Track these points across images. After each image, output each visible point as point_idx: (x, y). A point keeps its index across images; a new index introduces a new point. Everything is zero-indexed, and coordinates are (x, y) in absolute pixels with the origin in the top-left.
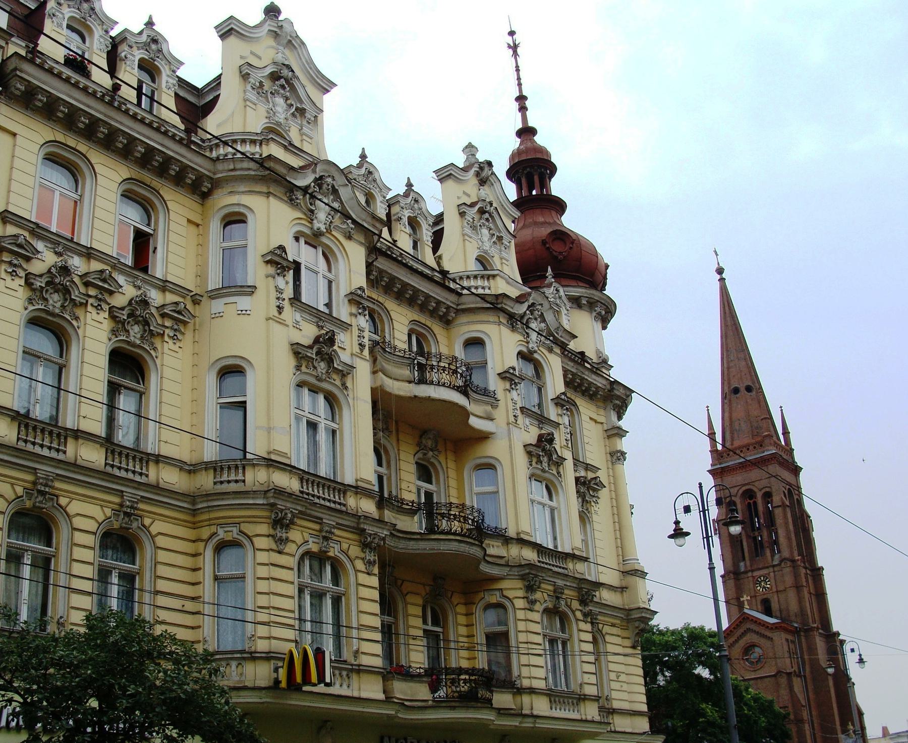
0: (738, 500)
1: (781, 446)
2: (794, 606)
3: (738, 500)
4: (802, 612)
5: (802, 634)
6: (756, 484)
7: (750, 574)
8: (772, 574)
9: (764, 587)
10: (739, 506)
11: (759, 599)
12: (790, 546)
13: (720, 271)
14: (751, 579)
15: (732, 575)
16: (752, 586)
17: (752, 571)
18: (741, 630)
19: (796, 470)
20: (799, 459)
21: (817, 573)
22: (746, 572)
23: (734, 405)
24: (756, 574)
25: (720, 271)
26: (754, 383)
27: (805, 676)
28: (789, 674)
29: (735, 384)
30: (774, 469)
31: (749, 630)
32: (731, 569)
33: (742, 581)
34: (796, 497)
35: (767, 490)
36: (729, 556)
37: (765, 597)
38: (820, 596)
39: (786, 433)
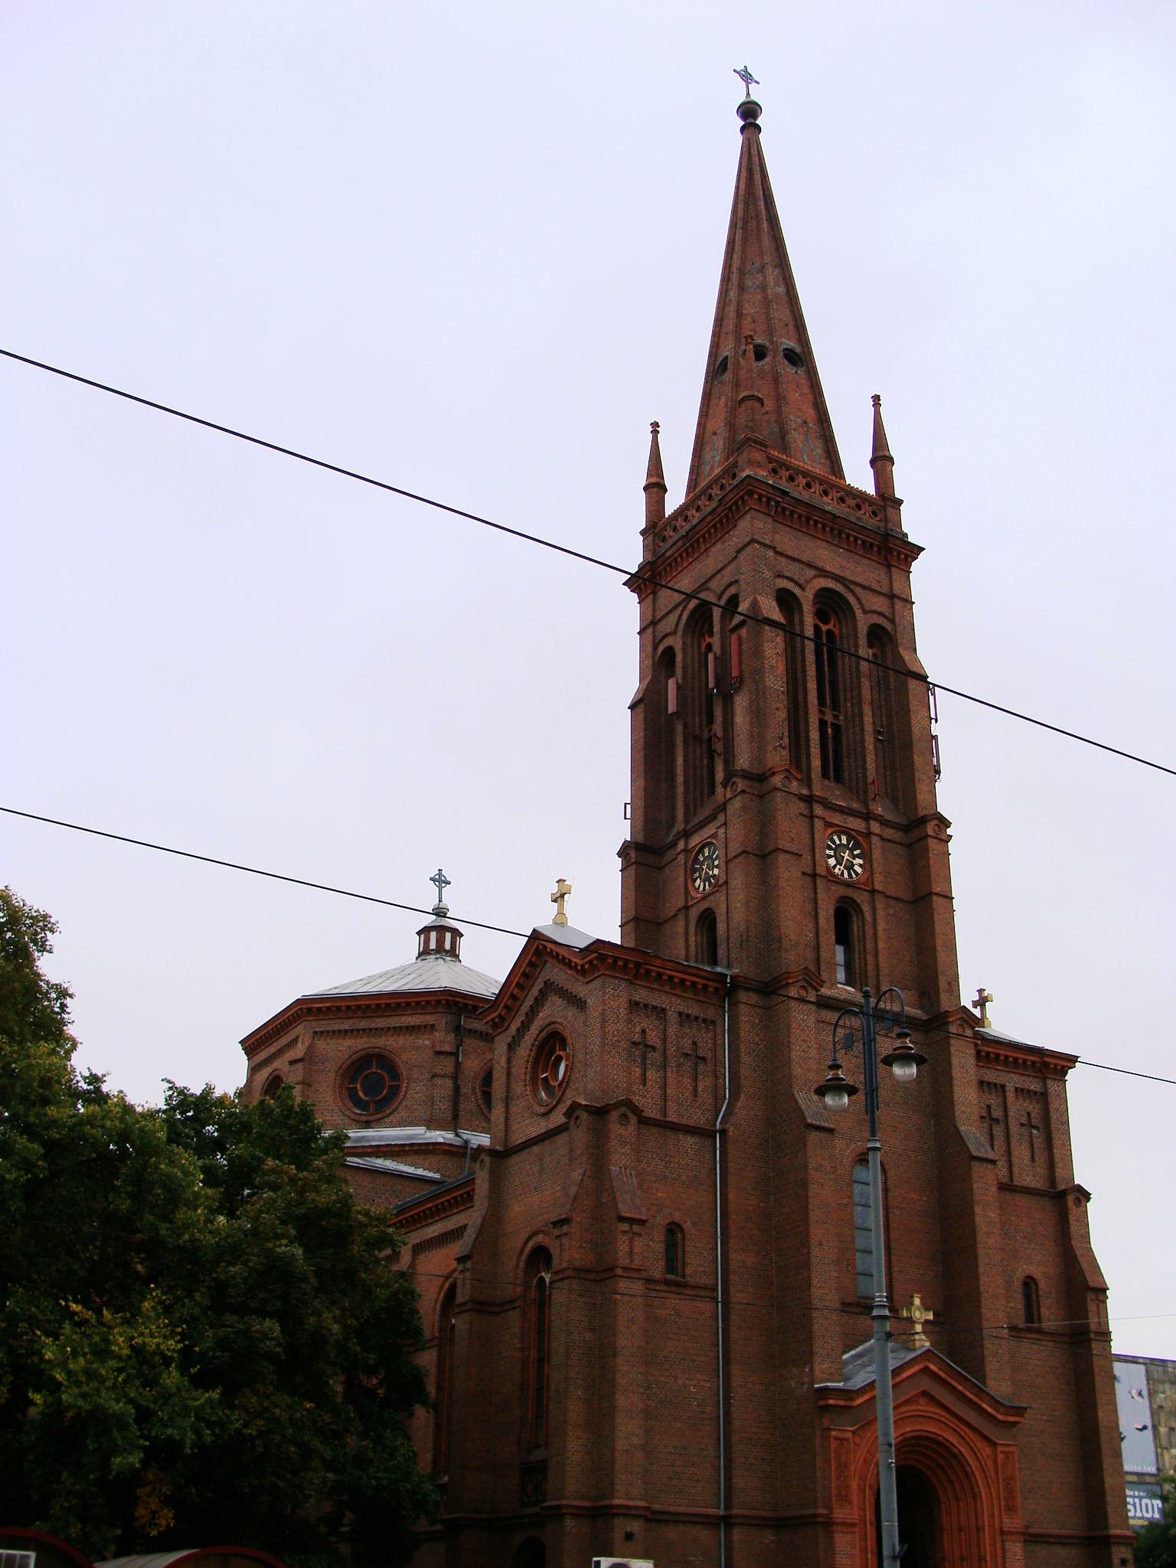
0: (676, 642)
1: (860, 496)
2: (736, 913)
3: (676, 642)
4: (766, 934)
5: (743, 996)
6: (713, 584)
7: (681, 845)
8: (722, 831)
9: (707, 879)
10: (679, 658)
11: (694, 914)
12: (758, 738)
13: (749, 112)
14: (681, 857)
15: (633, 854)
16: (682, 878)
17: (687, 834)
18: (535, 991)
19: (899, 553)
20: (913, 525)
21: (920, 836)
22: (674, 844)
23: (714, 401)
24: (695, 840)
25: (749, 112)
26: (770, 331)
27: (723, 1132)
28: (600, 1113)
29: (726, 351)
30: (753, 524)
31: (549, 987)
32: (640, 839)
33: (667, 870)
34: (863, 623)
35: (732, 590)
36: (641, 803)
37: (704, 905)
38: (924, 901)
39: (881, 460)
